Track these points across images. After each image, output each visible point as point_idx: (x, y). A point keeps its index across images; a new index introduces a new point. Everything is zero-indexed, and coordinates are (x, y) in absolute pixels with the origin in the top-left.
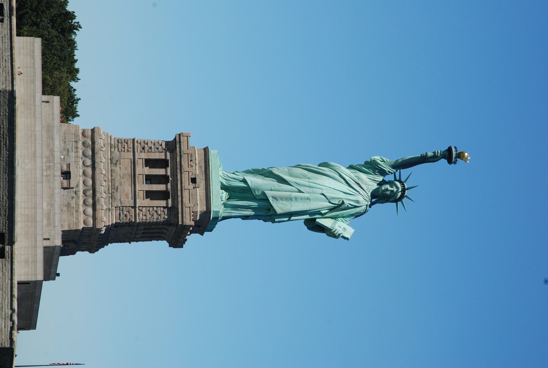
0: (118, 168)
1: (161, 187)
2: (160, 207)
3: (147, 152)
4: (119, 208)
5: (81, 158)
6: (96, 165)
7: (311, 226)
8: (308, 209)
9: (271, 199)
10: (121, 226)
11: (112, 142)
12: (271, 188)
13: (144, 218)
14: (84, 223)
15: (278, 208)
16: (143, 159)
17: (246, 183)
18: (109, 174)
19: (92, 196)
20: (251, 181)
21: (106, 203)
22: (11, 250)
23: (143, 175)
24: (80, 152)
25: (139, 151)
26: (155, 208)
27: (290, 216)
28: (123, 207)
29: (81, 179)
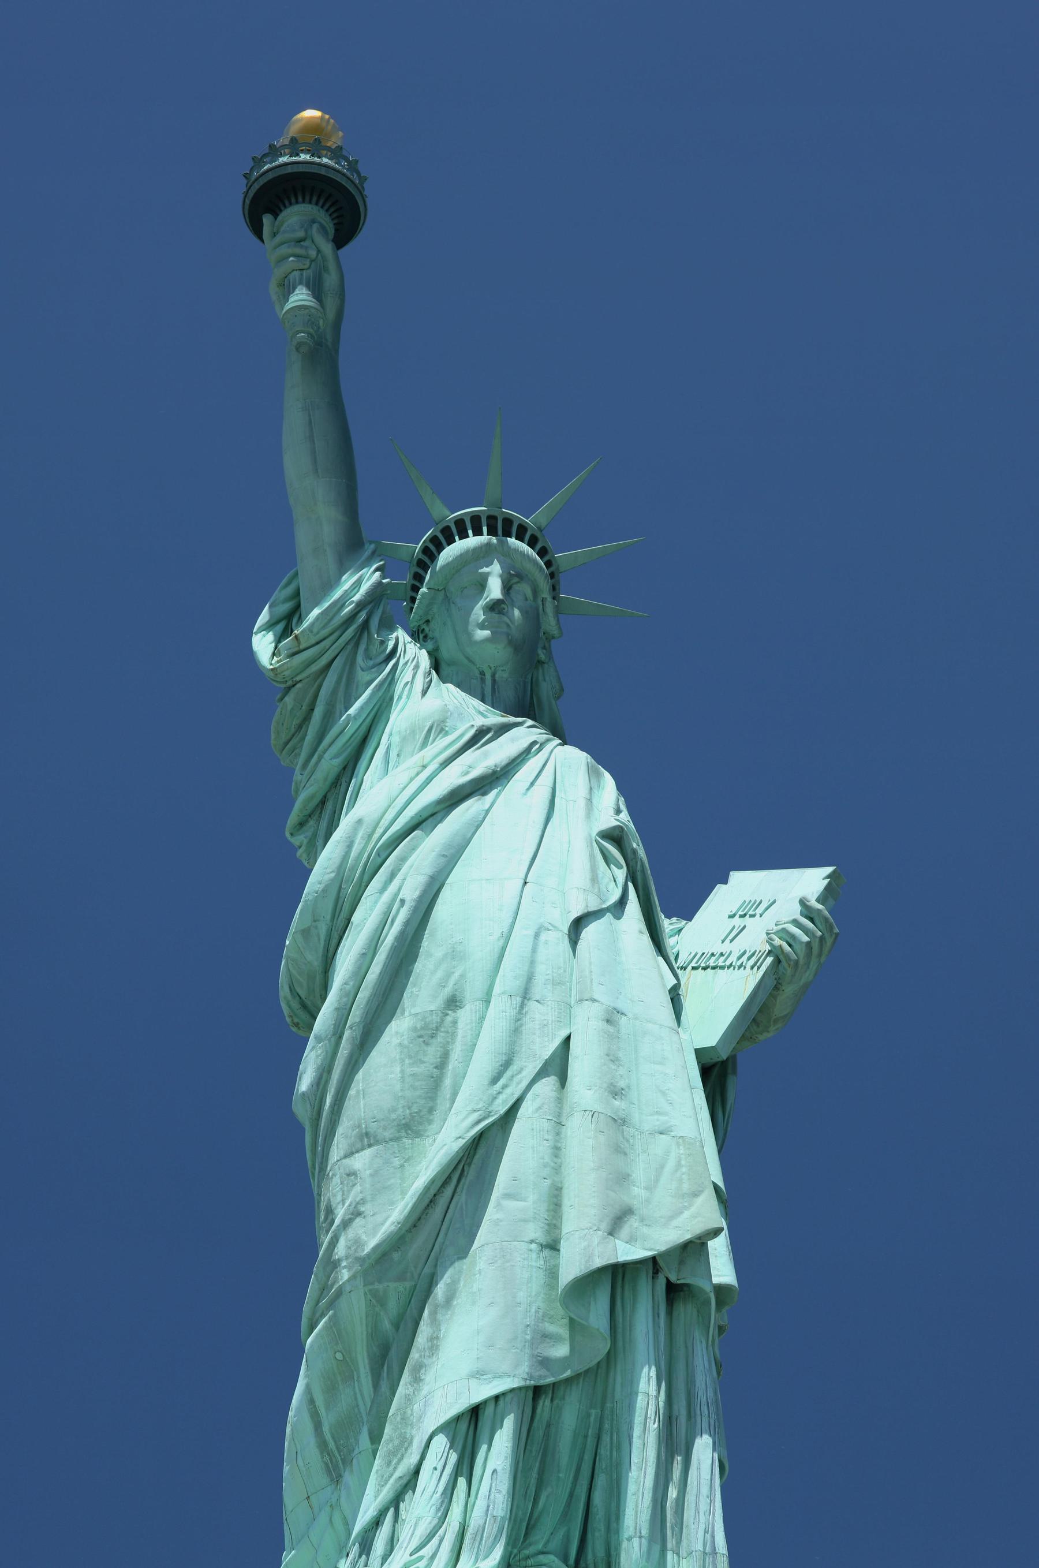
12: (533, 1246)
15: (687, 1214)
17: (490, 1410)
20: (478, 1374)
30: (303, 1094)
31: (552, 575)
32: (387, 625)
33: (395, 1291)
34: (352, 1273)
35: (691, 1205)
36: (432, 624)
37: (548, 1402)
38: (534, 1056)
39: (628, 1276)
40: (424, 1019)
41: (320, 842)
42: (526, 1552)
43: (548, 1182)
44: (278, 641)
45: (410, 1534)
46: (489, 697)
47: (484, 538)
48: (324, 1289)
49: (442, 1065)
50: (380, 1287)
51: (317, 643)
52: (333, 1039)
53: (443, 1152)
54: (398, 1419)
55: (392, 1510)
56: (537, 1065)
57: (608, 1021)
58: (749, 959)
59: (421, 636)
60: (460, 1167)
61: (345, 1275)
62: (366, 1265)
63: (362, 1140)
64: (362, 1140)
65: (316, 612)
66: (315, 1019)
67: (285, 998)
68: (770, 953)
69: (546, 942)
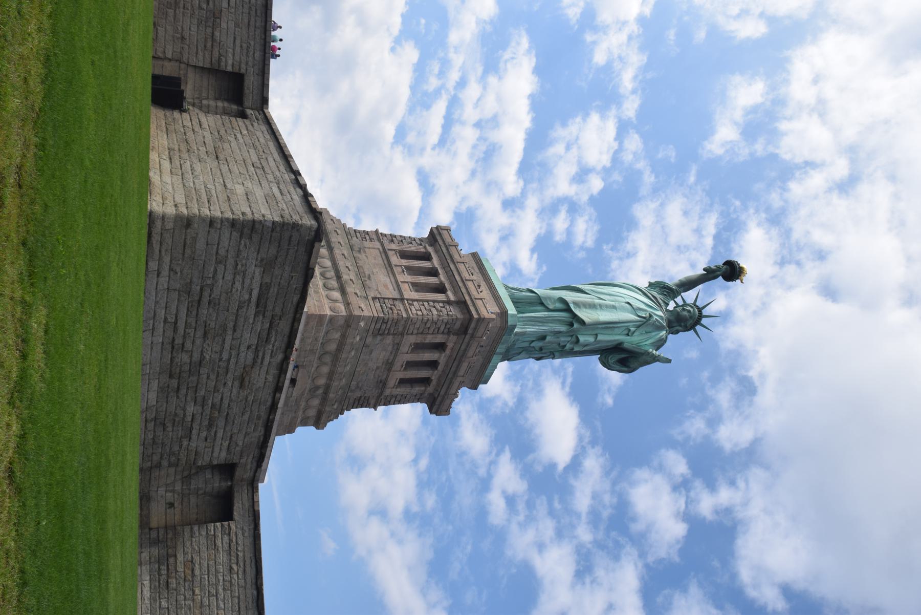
0: (364, 256)
1: (432, 280)
2: (439, 302)
4: (379, 300)
6: (333, 245)
7: (612, 362)
8: (617, 320)
10: (380, 334)
13: (419, 313)
14: (331, 310)
16: (394, 250)
19: (335, 278)
22: (260, 114)
23: (401, 266)
26: (431, 303)
27: (594, 336)
28: (384, 298)
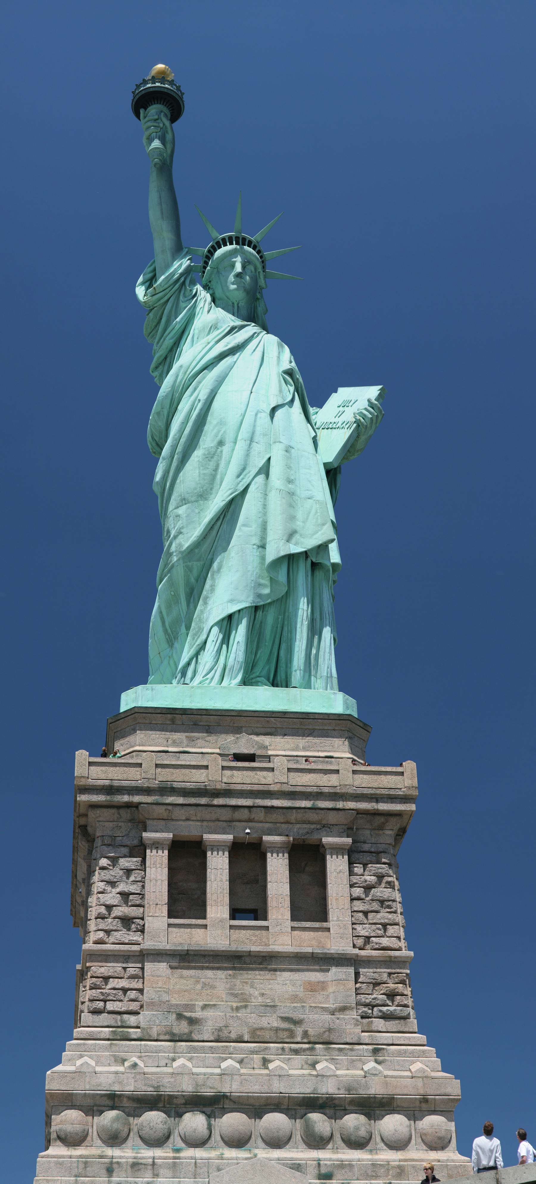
0: (209, 1014)
3: (141, 909)
4: (362, 1017)
5: (178, 1151)
9: (295, 549)
11: (102, 1031)
12: (255, 547)
13: (391, 930)
15: (320, 533)
16: (169, 925)
17: (236, 616)
18: (234, 1047)
20: (231, 601)
21: (353, 1061)
24: (148, 1153)
25: (136, 937)
28: (359, 1004)
29: (264, 1153)
30: (157, 482)
31: (263, 262)
32: (193, 283)
33: (196, 566)
34: (178, 558)
35: (322, 529)
36: (212, 283)
37: (261, 613)
38: (255, 466)
39: (295, 560)
40: (208, 450)
41: (164, 376)
42: (252, 676)
43: (261, 519)
44: (147, 290)
45: (202, 669)
46: (236, 313)
47: (234, 246)
48: (166, 565)
49: (216, 470)
50: (190, 564)
51: (163, 291)
52: (170, 459)
53: (216, 507)
54: (198, 620)
55: (195, 659)
56: (257, 469)
57: (286, 451)
58: (346, 424)
59: (207, 288)
60: (224, 513)
61: (175, 559)
62: (184, 554)
63: (182, 502)
64: (182, 502)
65: (163, 277)
66: (162, 450)
67: (150, 441)
68: (355, 422)
69: (260, 418)
